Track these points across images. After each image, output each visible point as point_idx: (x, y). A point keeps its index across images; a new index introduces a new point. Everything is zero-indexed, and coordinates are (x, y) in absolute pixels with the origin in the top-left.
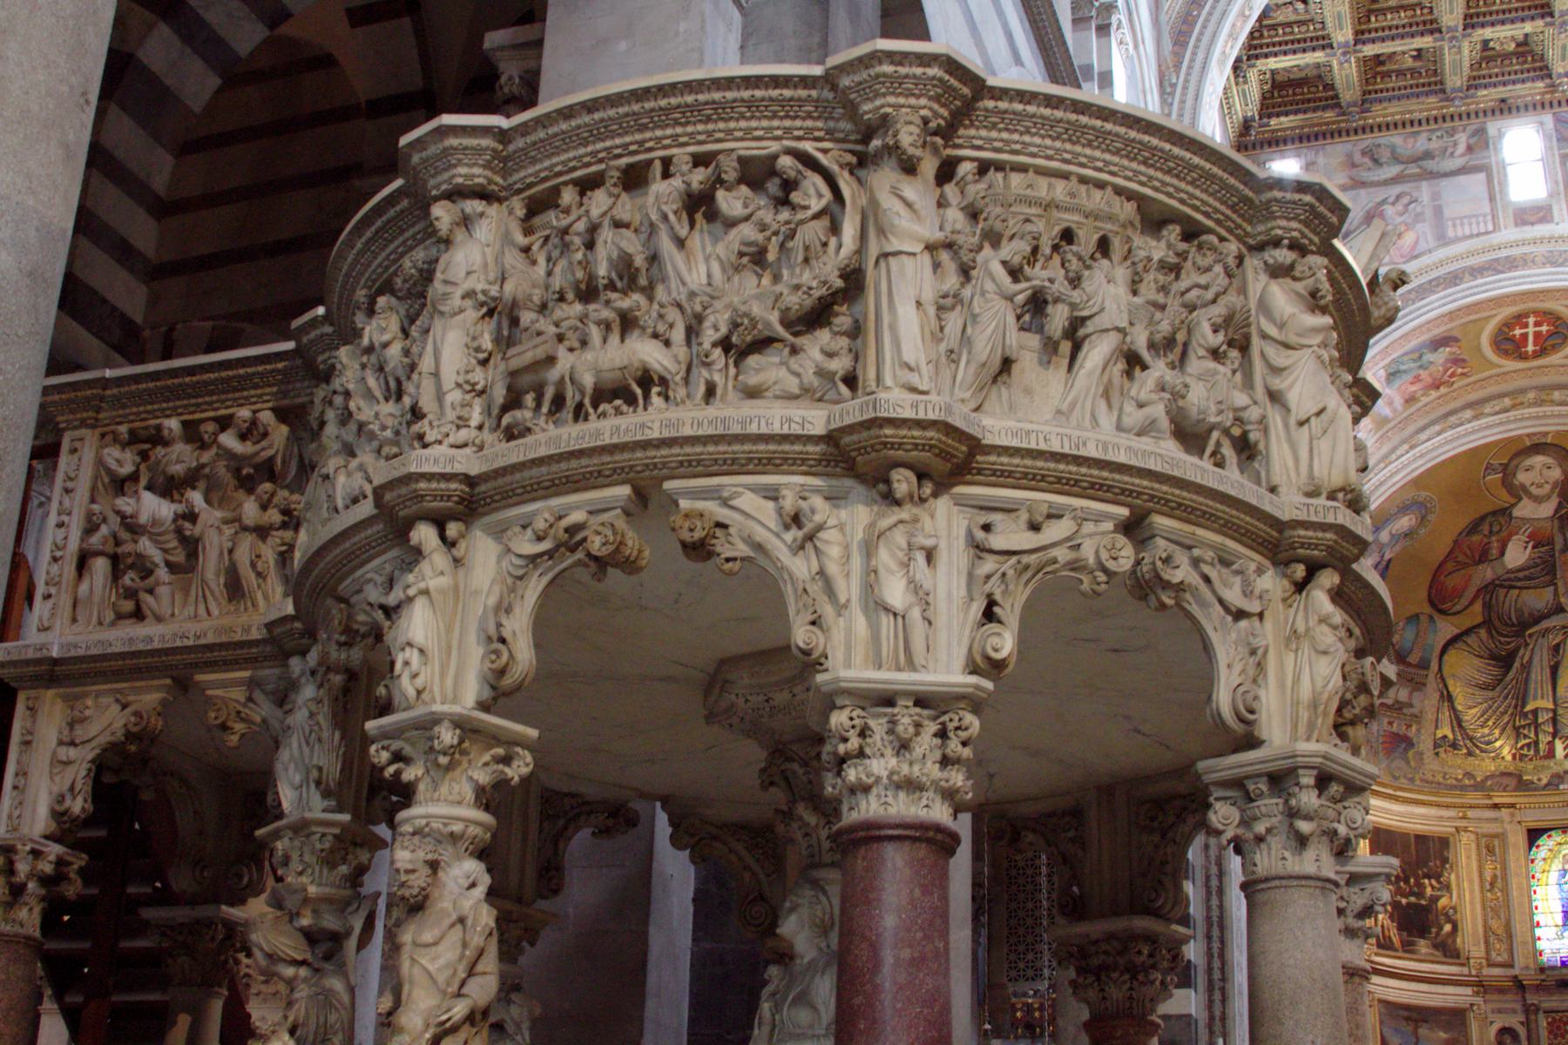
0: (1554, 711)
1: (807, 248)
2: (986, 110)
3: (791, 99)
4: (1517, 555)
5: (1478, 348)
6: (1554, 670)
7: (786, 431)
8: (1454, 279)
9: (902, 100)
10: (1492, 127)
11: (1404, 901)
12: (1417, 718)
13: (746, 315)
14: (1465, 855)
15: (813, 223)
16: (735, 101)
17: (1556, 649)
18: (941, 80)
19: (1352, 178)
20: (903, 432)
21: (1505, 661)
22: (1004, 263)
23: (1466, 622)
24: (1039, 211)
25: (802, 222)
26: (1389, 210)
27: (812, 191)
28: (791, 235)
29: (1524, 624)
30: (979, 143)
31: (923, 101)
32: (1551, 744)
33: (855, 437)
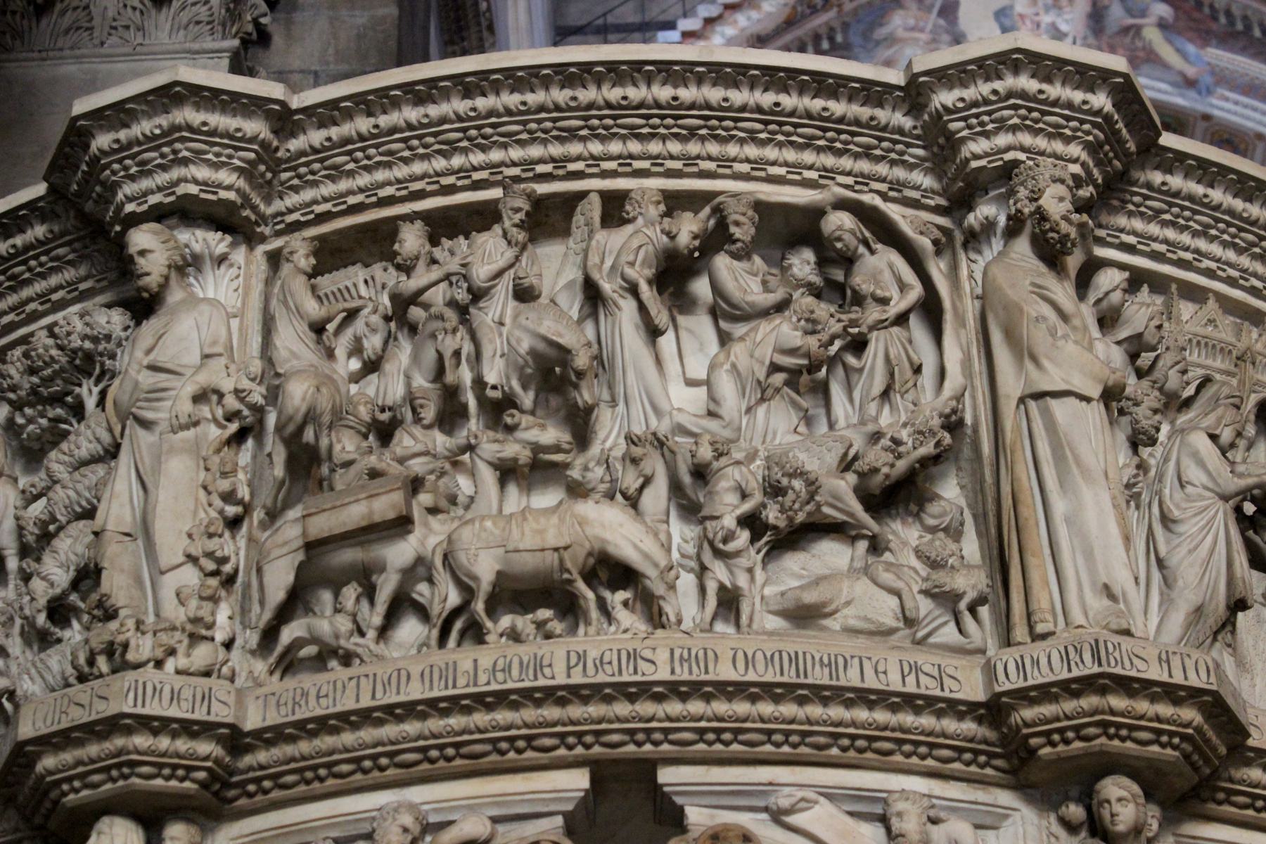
2: (1149, 186)
3: (841, 120)
7: (911, 688)
9: (1041, 143)
16: (743, 108)
24: (1227, 365)
31: (1075, 150)
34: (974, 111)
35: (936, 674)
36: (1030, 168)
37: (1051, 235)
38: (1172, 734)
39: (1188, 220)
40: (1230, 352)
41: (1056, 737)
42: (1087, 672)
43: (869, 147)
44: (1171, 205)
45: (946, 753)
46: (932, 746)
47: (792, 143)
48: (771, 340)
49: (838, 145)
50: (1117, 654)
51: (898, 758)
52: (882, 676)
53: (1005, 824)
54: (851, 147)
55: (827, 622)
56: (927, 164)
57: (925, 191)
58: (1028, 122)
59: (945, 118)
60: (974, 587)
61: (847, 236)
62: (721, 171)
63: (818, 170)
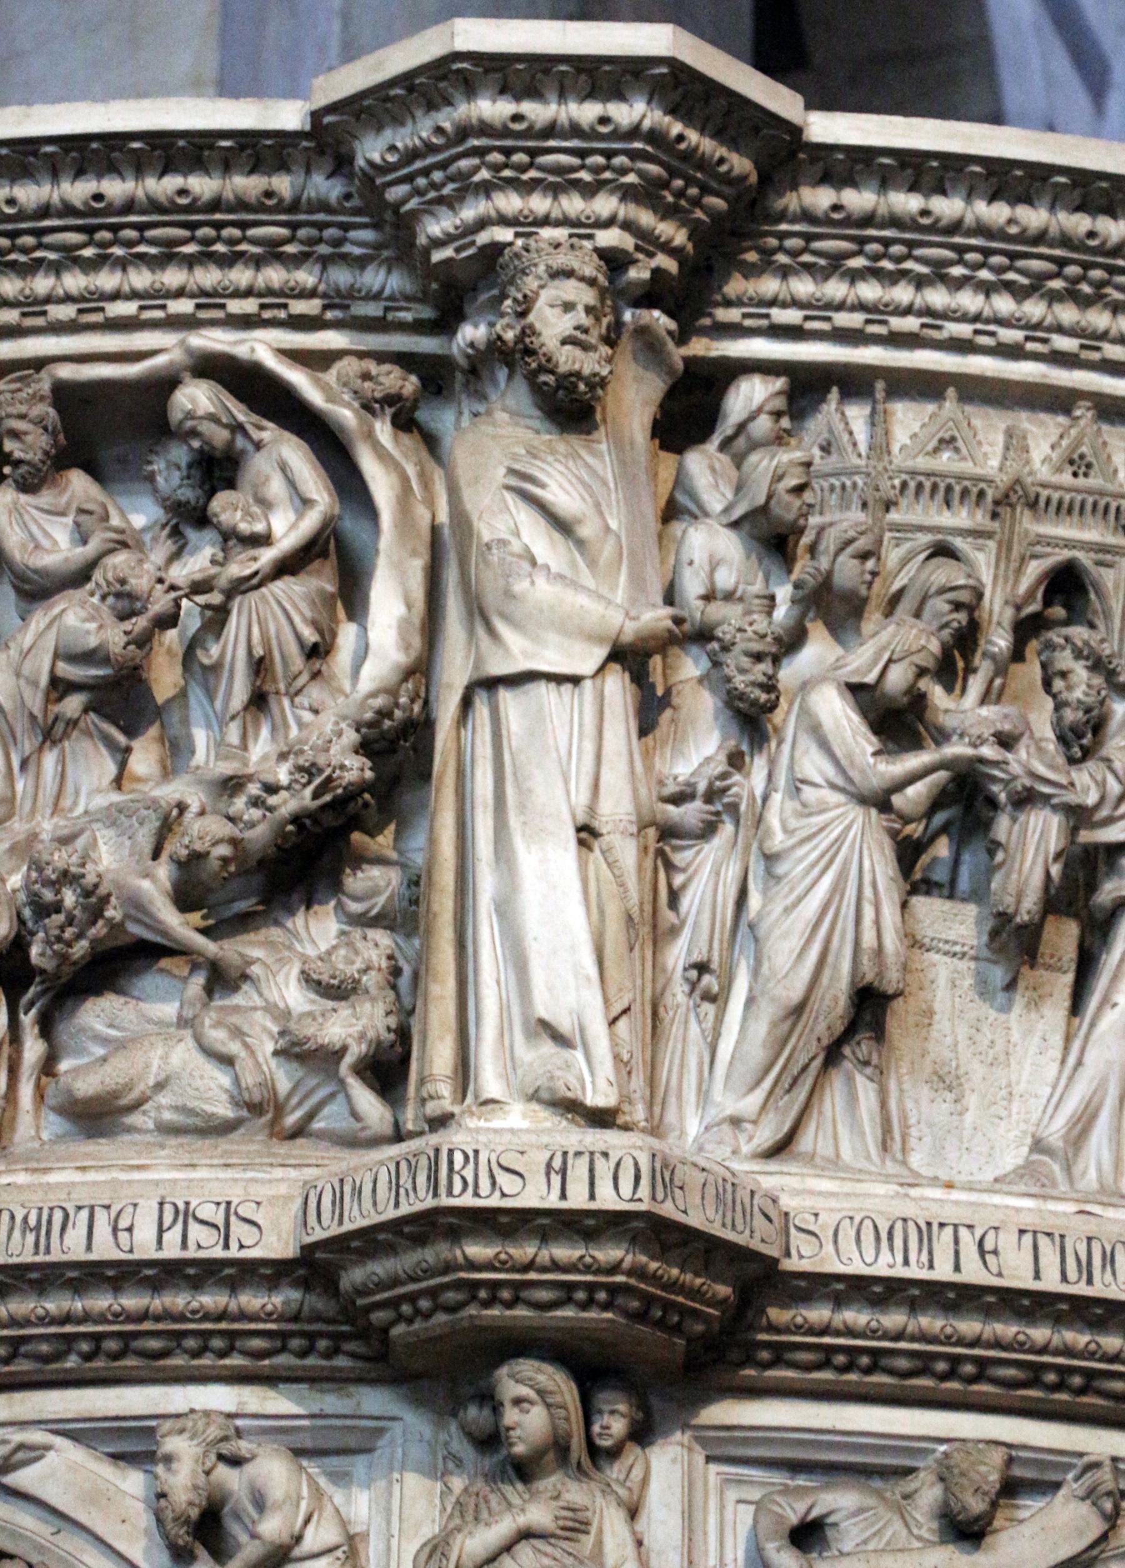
1: (259, 666)
2: (807, 216)
3: (216, 204)
7: (172, 1250)
9: (540, 204)
13: (67, 877)
15: (279, 587)
16: (45, 211)
18: (655, 136)
20: (524, 1251)
22: (856, 690)
24: (980, 519)
25: (241, 587)
27: (276, 487)
28: (216, 620)
30: (791, 316)
31: (605, 205)
33: (380, 1268)
34: (418, 164)
35: (220, 1221)
36: (517, 255)
37: (544, 378)
38: (591, 1287)
39: (898, 260)
40: (981, 494)
41: (406, 1309)
42: (419, 1207)
43: (273, 244)
44: (862, 241)
45: (257, 1343)
46: (232, 1335)
47: (141, 257)
48: (50, 643)
49: (220, 248)
50: (468, 1173)
51: (178, 1361)
52: (123, 1236)
53: (380, 1443)
54: (243, 247)
55: (134, 1119)
56: (386, 253)
57: (391, 298)
58: (507, 173)
59: (379, 181)
60: (362, 1036)
61: (206, 428)
62: (29, 322)
63: (192, 296)
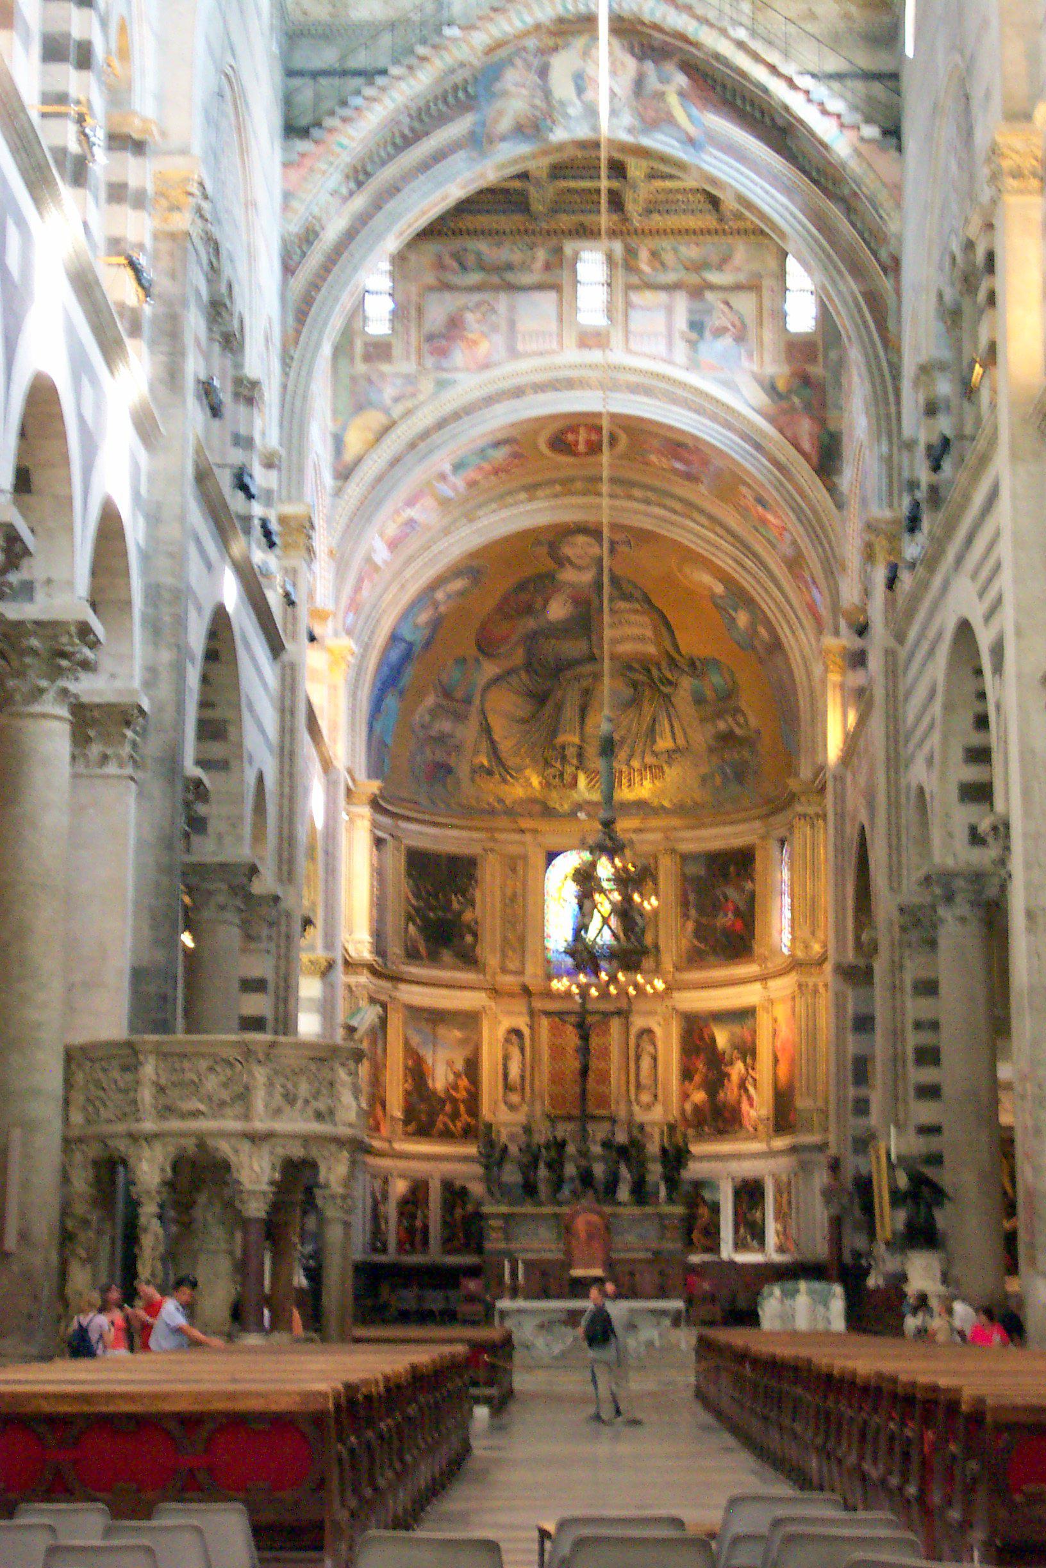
0: (580, 747)
4: (558, 610)
5: (536, 448)
6: (583, 711)
8: (518, 392)
10: (569, 247)
11: (432, 915)
12: (458, 748)
14: (491, 874)
17: (587, 693)
19: (440, 281)
21: (540, 699)
23: (507, 664)
26: (470, 317)
29: (559, 669)
32: (575, 778)
